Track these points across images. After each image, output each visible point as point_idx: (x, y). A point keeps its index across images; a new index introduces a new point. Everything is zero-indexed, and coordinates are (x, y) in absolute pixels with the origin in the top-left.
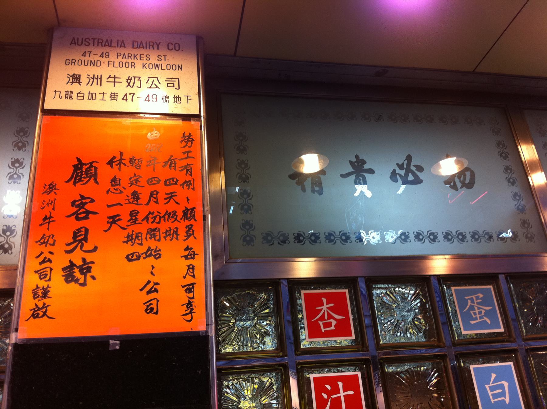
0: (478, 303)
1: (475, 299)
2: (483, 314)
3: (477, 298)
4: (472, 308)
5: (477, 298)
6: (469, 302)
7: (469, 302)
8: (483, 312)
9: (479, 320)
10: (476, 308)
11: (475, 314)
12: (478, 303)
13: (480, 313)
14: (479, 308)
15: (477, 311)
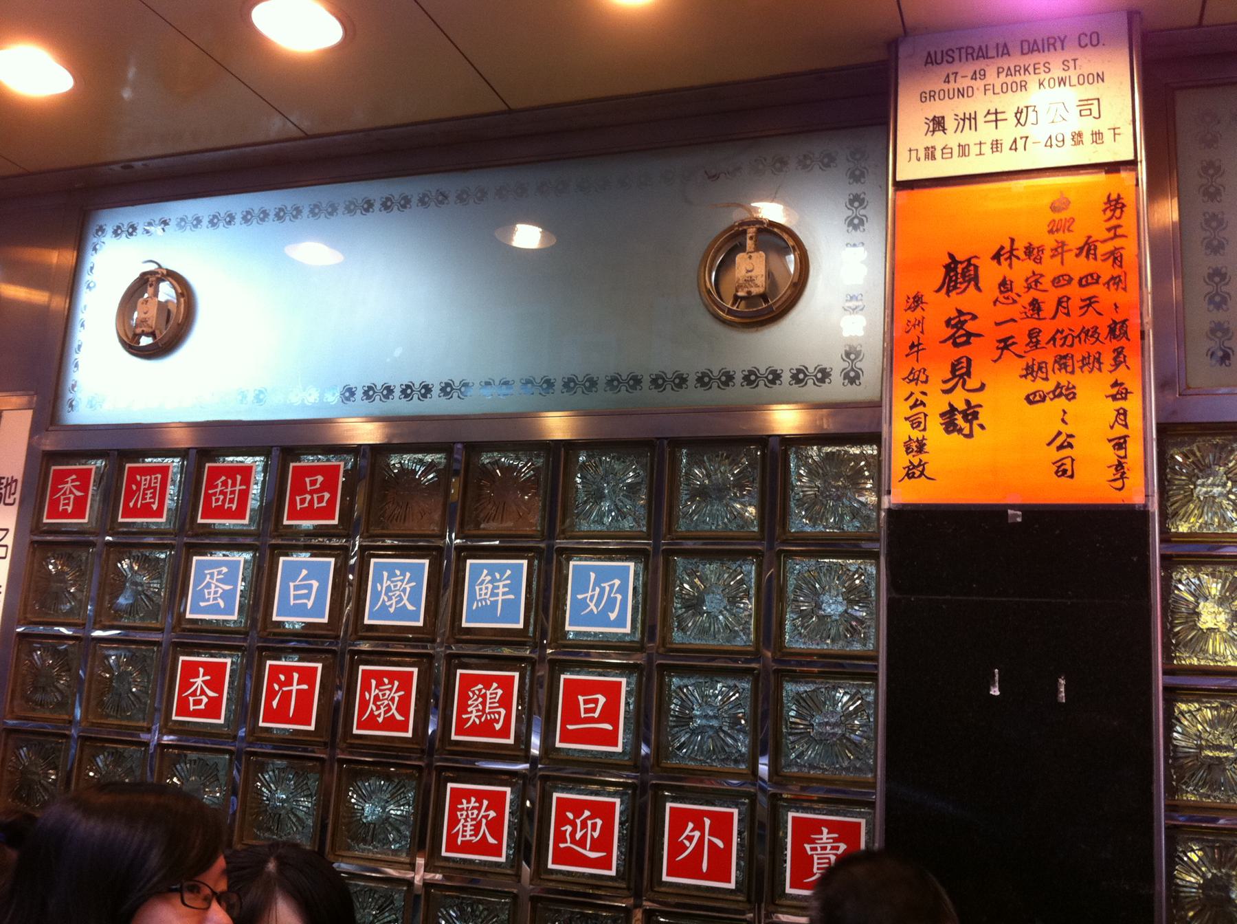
0: (217, 580)
1: (216, 573)
2: (219, 595)
3: (219, 573)
4: (208, 586)
5: (219, 573)
6: (208, 576)
7: (208, 576)
8: (220, 591)
9: (211, 602)
10: (213, 586)
11: (209, 593)
12: (217, 580)
13: (216, 592)
14: (216, 587)
15: (212, 590)
